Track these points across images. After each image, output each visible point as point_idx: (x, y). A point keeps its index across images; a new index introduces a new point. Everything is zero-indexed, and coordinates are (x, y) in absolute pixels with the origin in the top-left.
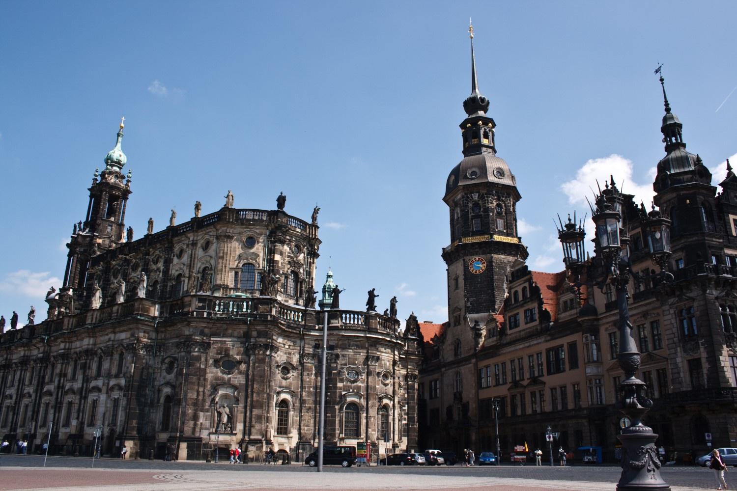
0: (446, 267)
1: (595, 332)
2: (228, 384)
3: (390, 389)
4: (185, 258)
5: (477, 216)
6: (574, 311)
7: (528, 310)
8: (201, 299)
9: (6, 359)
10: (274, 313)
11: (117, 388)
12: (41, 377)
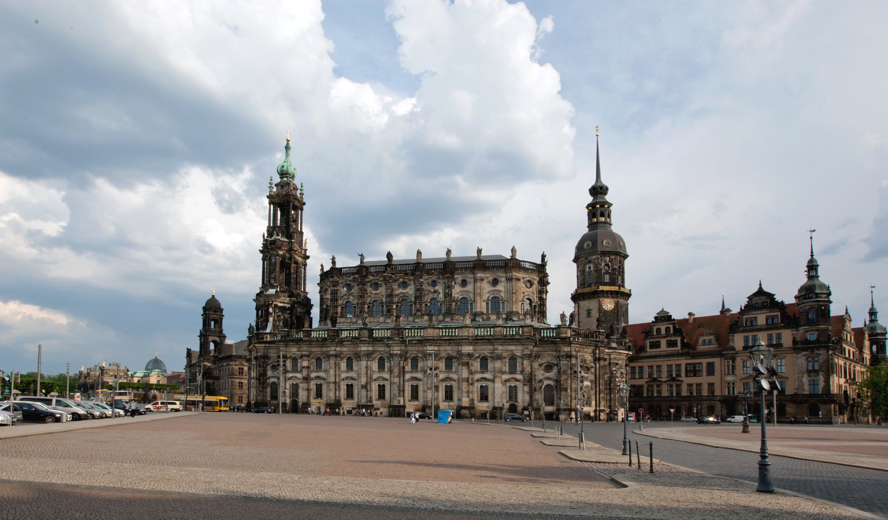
1: (734, 361)
2: (587, 379)
5: (607, 273)
6: (713, 346)
7: (671, 340)
9: (335, 350)
11: (514, 380)
12: (401, 368)
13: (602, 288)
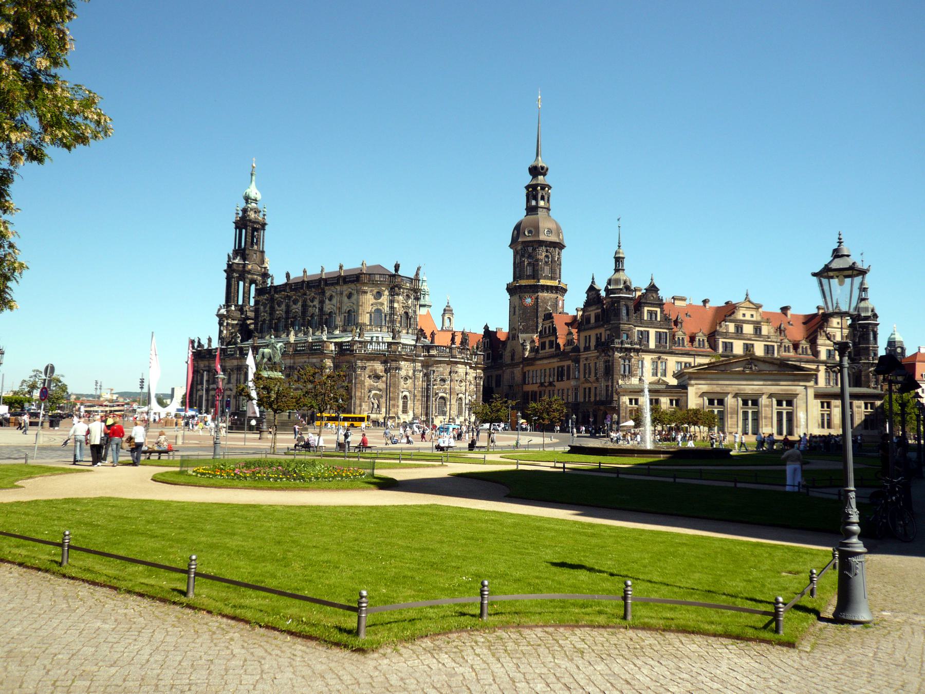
0: (508, 297)
1: (577, 361)
3: (464, 388)
4: (334, 301)
8: (360, 342)
10: (399, 350)
13: (524, 282)
